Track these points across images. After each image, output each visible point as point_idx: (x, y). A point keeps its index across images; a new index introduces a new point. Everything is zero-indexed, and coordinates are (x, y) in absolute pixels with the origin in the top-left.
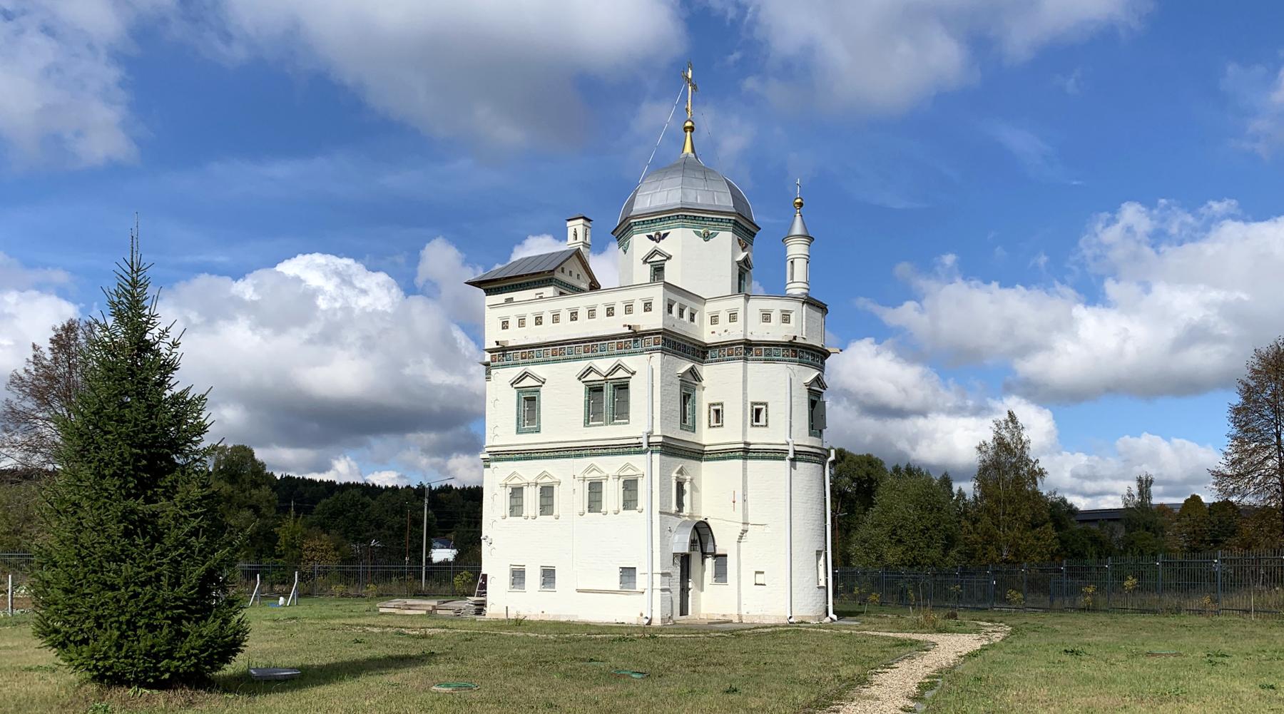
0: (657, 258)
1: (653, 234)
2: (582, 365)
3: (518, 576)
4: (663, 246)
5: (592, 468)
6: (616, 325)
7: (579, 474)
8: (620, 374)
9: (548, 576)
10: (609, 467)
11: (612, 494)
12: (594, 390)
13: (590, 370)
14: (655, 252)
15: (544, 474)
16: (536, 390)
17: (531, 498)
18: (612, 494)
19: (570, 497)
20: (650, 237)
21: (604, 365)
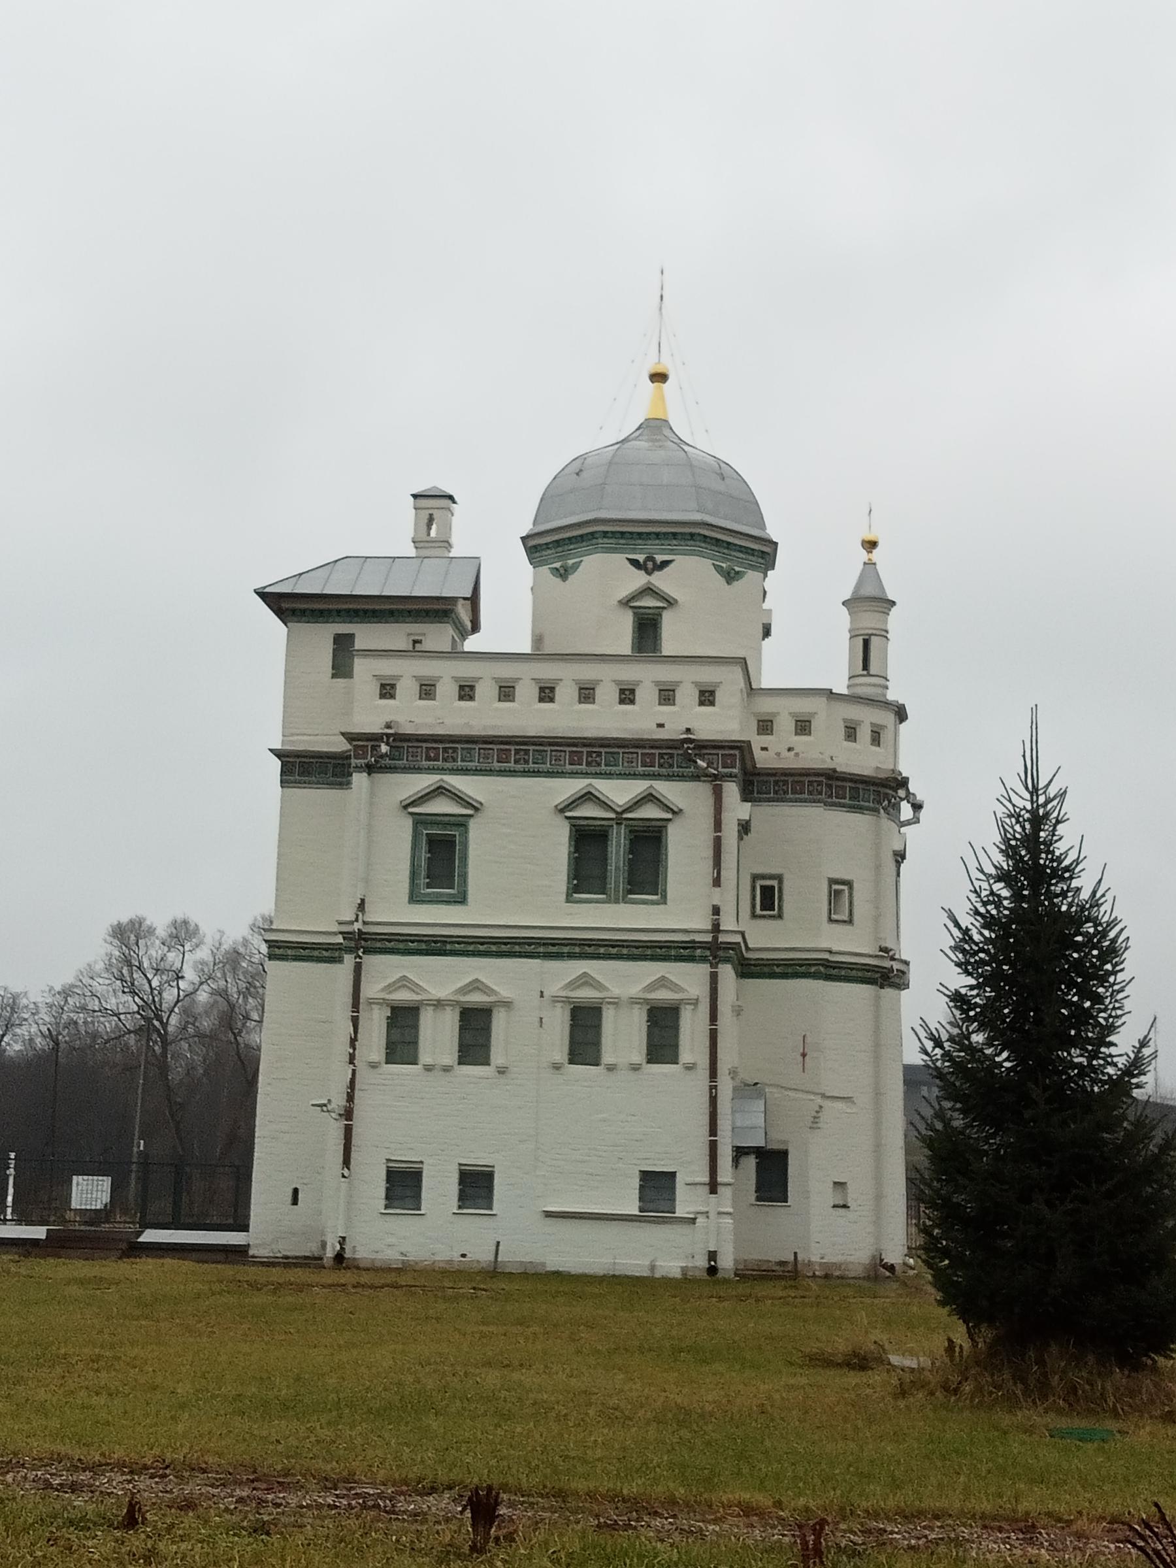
0: (649, 602)
1: (641, 558)
2: (572, 787)
3: (404, 1185)
4: (659, 580)
5: (585, 980)
6: (642, 720)
7: (555, 988)
8: (650, 812)
9: (476, 1186)
11: (624, 1035)
13: (588, 797)
14: (649, 591)
15: (476, 986)
16: (461, 823)
17: (438, 1035)
18: (624, 1035)
20: (635, 563)
21: (620, 792)
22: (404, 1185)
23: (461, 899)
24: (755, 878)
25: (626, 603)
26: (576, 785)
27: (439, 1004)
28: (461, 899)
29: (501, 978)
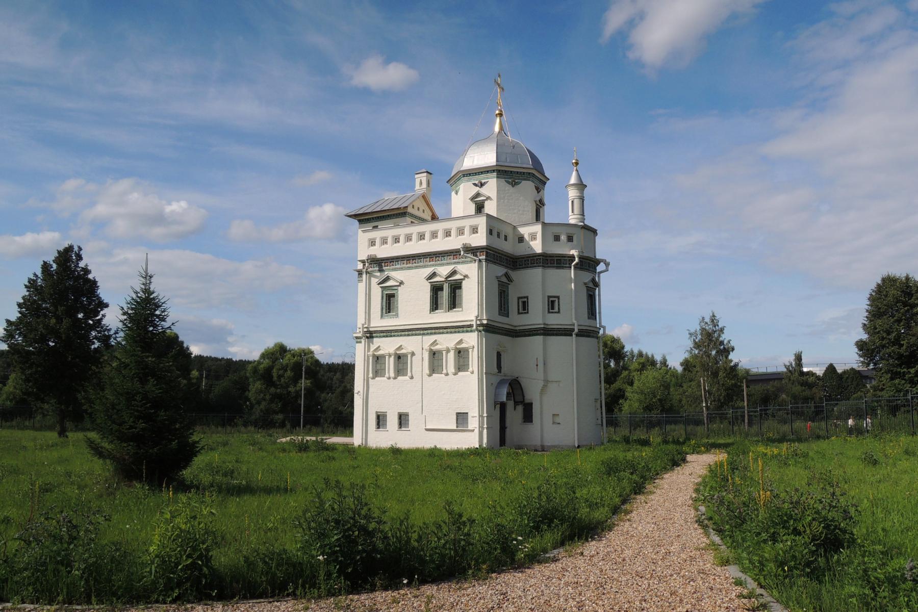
3: (381, 420)
5: (435, 343)
8: (457, 277)
9: (403, 420)
10: (447, 341)
12: (436, 290)
13: (434, 275)
14: (478, 195)
19: (419, 364)
20: (475, 185)
21: (443, 271)
22: (381, 420)
23: (397, 315)
24: (519, 298)
25: (472, 199)
26: (428, 271)
27: (390, 356)
28: (397, 315)
29: (409, 344)
